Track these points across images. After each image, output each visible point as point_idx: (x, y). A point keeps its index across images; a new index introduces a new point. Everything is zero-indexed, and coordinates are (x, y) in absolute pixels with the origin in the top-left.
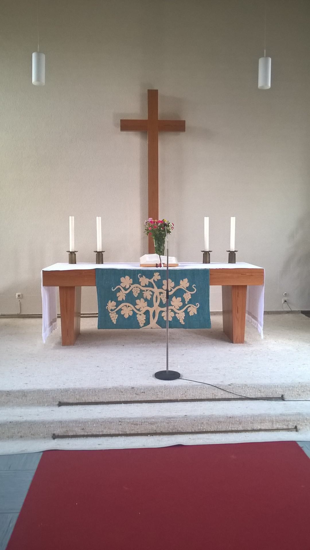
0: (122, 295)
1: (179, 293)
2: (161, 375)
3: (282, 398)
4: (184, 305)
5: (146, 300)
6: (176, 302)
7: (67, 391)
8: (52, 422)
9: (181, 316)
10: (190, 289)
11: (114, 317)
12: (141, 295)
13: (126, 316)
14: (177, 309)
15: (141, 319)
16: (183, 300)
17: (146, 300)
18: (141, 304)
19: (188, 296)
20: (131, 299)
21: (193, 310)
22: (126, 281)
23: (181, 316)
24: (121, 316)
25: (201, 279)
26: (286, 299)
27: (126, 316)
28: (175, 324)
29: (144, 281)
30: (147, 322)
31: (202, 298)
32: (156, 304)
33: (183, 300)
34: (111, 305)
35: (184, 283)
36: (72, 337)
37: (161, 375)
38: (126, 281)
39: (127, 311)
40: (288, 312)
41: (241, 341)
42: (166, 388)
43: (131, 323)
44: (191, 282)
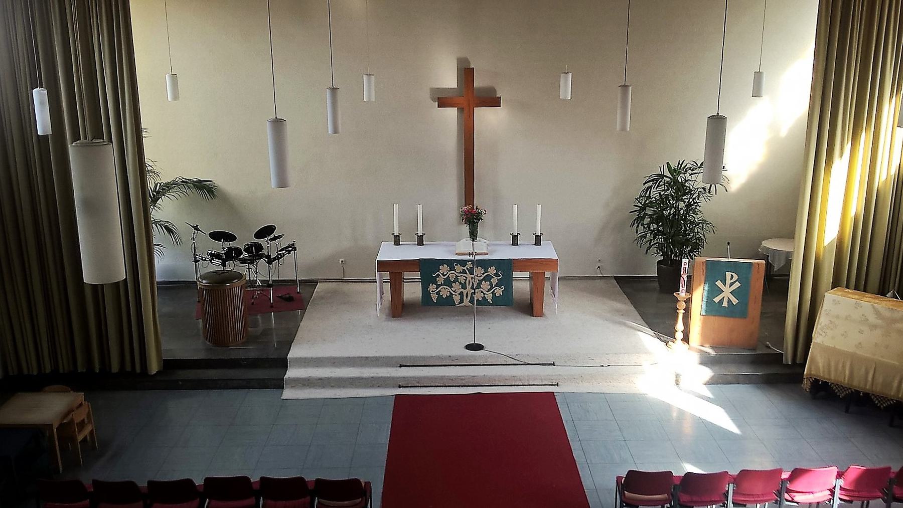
0: (440, 280)
1: (488, 278)
2: (470, 347)
3: (554, 364)
4: (492, 287)
5: (460, 283)
6: (485, 285)
7: (405, 357)
8: (398, 378)
9: (489, 296)
10: (496, 275)
11: (434, 297)
12: (456, 280)
13: (444, 296)
14: (486, 292)
15: (456, 298)
16: (491, 284)
17: (460, 283)
18: (456, 287)
19: (495, 281)
20: (448, 283)
21: (499, 291)
22: (444, 269)
23: (489, 296)
24: (440, 296)
25: (506, 267)
26: (599, 264)
27: (444, 296)
28: (483, 302)
29: (459, 268)
30: (462, 301)
31: (506, 281)
32: (469, 287)
33: (491, 284)
34: (432, 287)
35: (492, 271)
36: (400, 309)
37: (470, 347)
38: (444, 269)
39: (445, 293)
40: (600, 278)
41: (541, 315)
42: (473, 356)
43: (447, 302)
44: (497, 269)
